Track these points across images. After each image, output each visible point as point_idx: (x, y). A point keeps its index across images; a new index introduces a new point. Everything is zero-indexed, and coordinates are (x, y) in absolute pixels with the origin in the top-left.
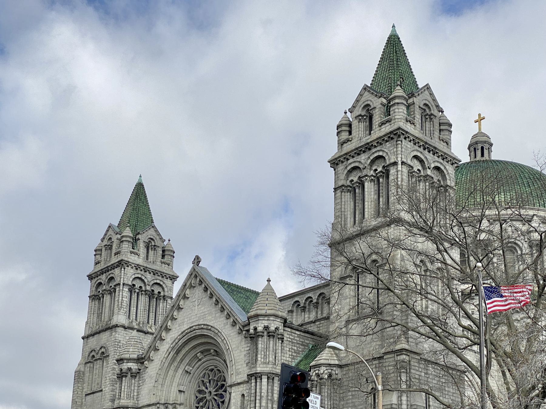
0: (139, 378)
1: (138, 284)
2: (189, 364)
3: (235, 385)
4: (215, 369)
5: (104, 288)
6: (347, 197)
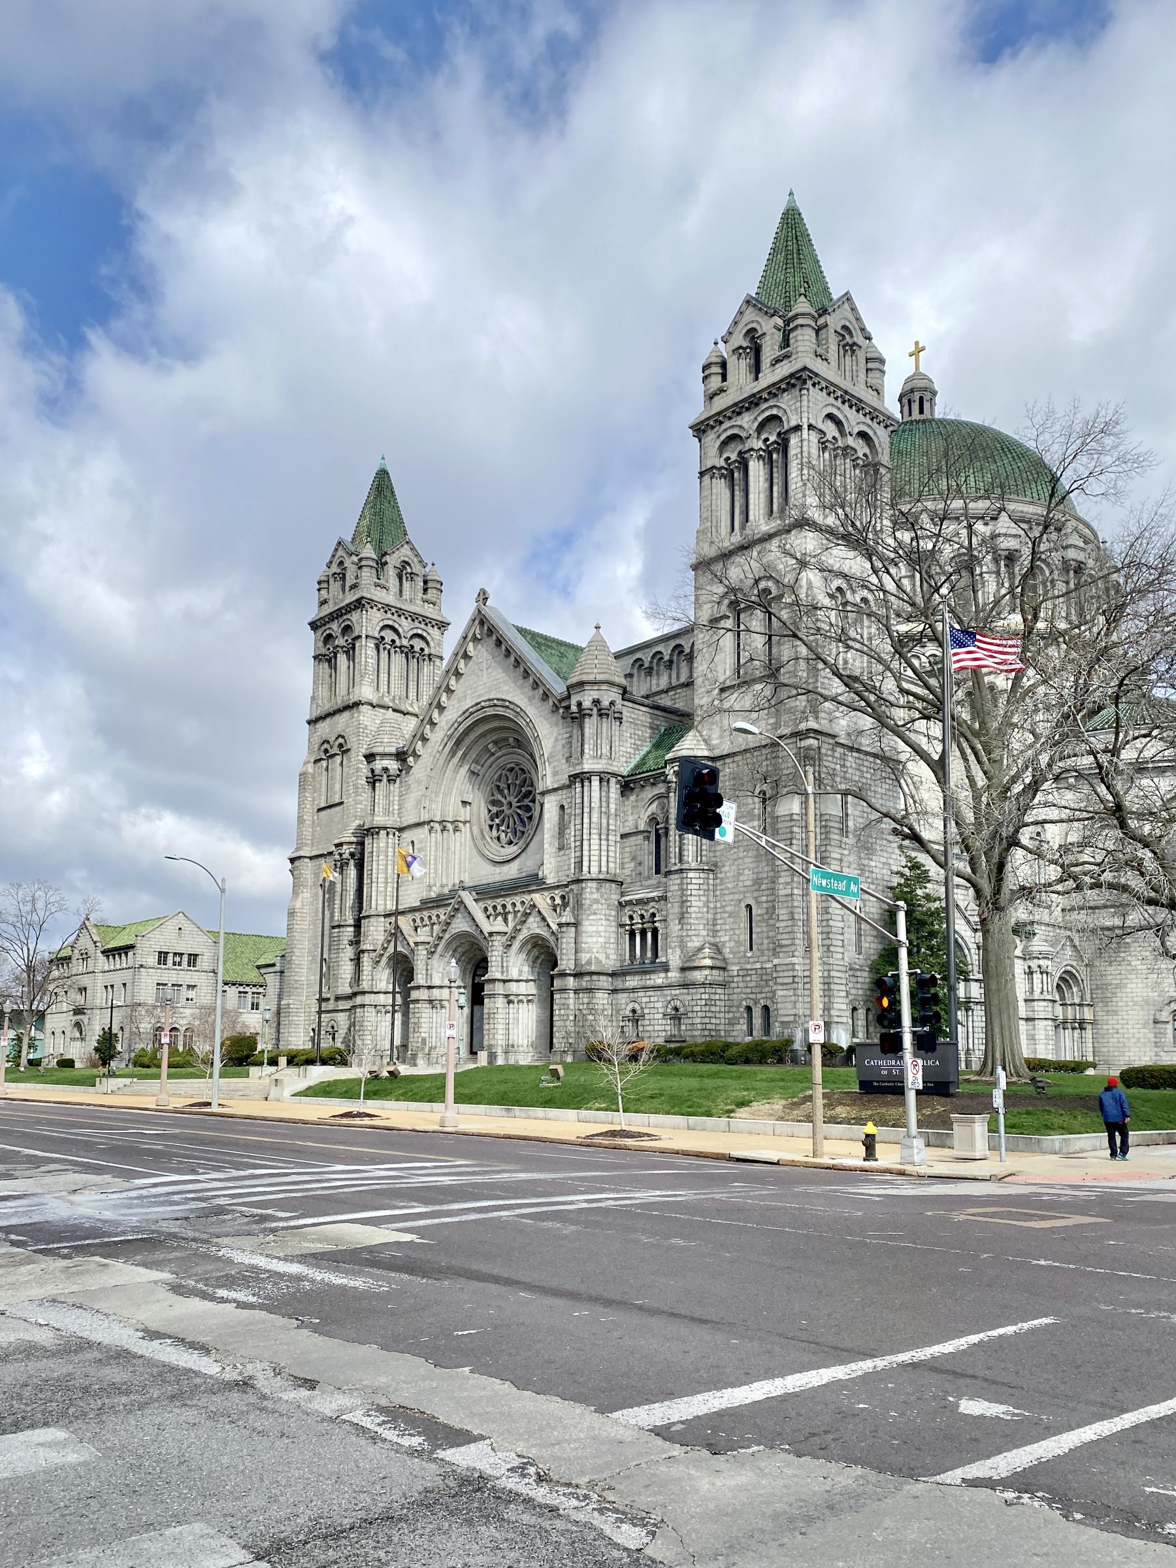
4: (517, 768)
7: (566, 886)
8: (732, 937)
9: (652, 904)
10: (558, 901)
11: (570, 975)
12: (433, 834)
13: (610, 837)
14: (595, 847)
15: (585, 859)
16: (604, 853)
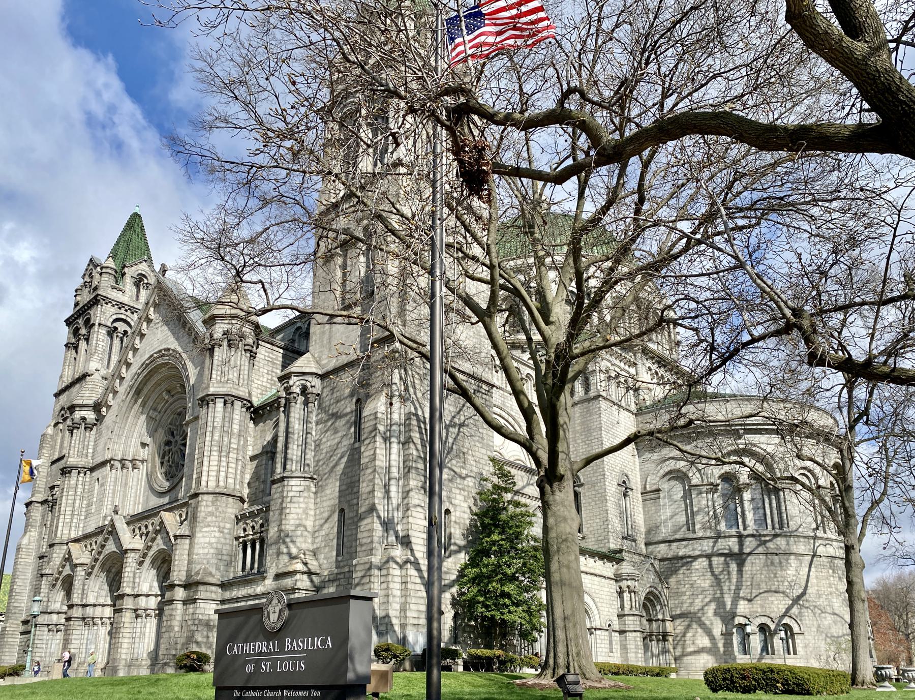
15: (205, 474)
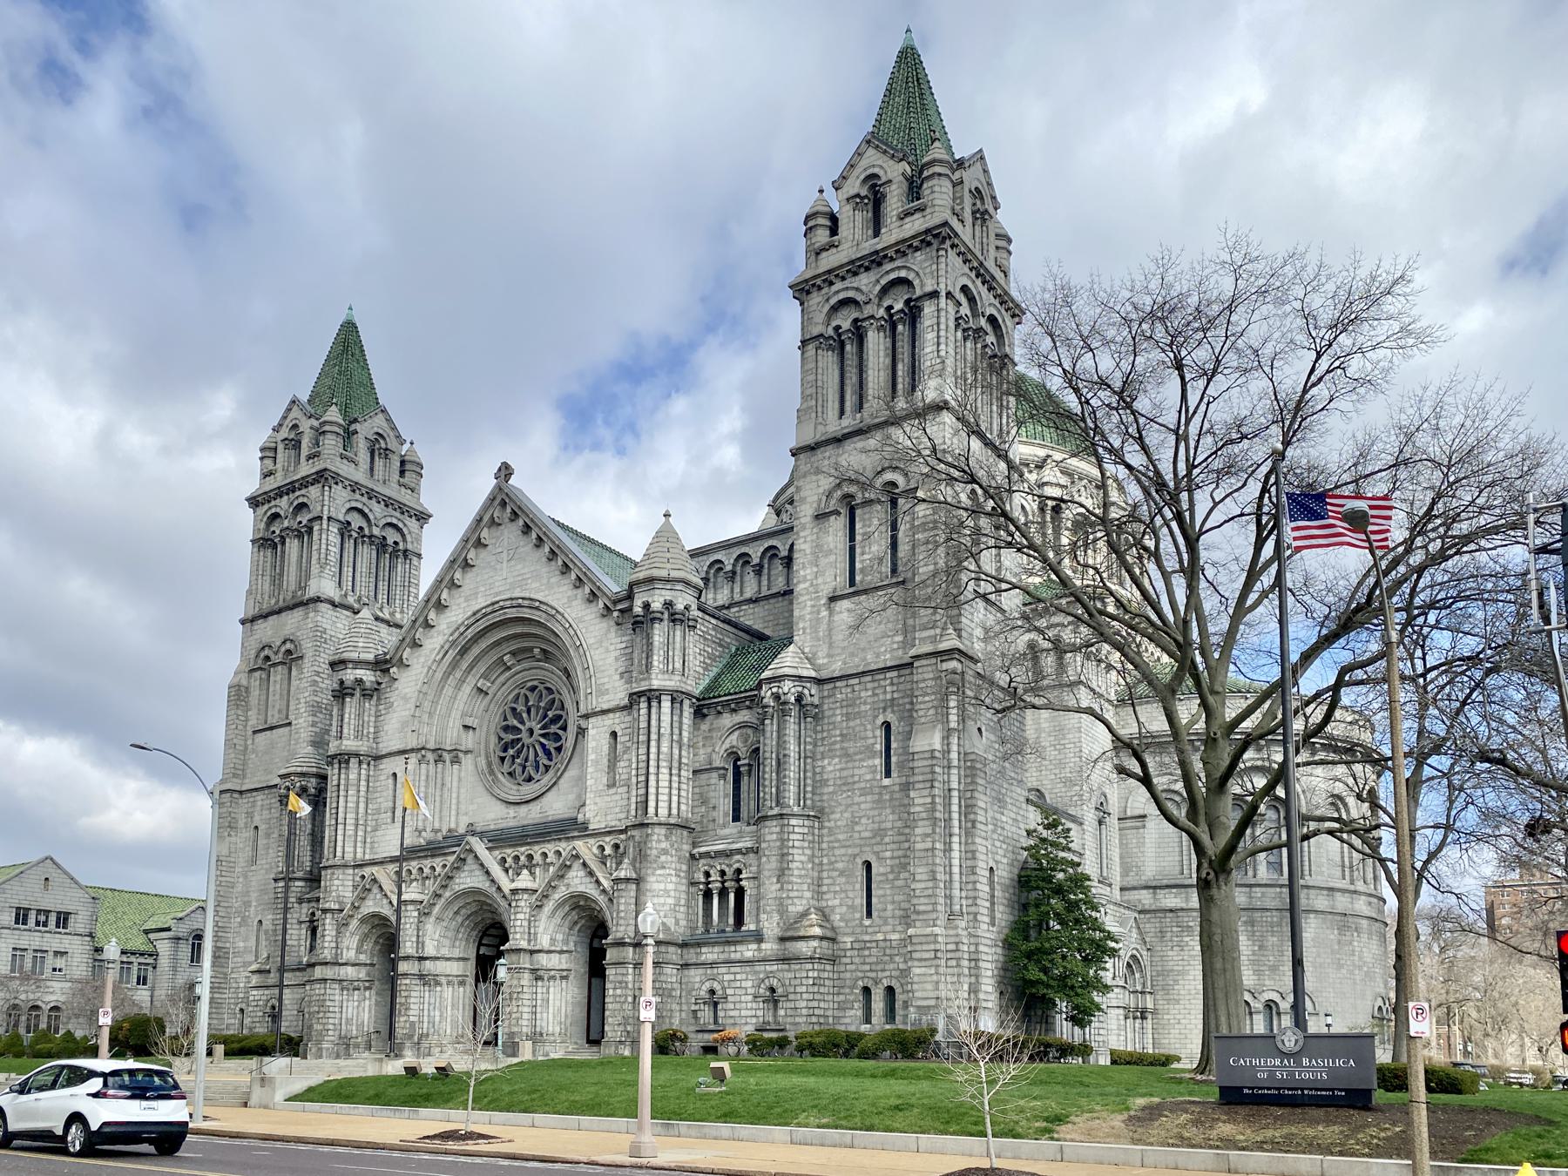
0: (379, 699)
1: (356, 521)
2: (485, 676)
3: (595, 714)
4: (541, 687)
5: (286, 524)
6: (829, 360)
7: (621, 832)
8: (844, 901)
9: (738, 857)
10: (608, 851)
11: (630, 944)
12: (423, 766)
13: (683, 773)
14: (664, 783)
15: (652, 798)
16: (675, 792)
